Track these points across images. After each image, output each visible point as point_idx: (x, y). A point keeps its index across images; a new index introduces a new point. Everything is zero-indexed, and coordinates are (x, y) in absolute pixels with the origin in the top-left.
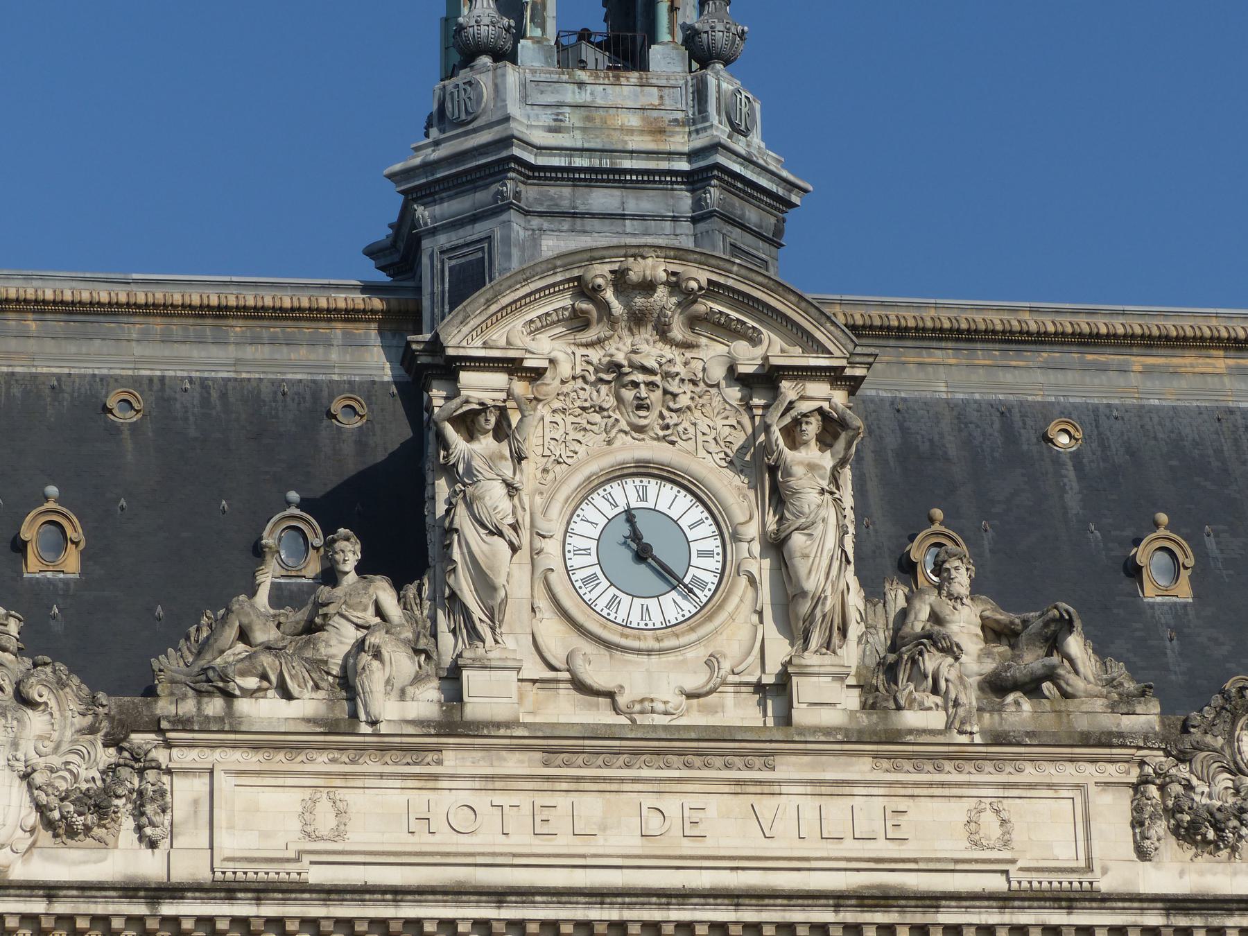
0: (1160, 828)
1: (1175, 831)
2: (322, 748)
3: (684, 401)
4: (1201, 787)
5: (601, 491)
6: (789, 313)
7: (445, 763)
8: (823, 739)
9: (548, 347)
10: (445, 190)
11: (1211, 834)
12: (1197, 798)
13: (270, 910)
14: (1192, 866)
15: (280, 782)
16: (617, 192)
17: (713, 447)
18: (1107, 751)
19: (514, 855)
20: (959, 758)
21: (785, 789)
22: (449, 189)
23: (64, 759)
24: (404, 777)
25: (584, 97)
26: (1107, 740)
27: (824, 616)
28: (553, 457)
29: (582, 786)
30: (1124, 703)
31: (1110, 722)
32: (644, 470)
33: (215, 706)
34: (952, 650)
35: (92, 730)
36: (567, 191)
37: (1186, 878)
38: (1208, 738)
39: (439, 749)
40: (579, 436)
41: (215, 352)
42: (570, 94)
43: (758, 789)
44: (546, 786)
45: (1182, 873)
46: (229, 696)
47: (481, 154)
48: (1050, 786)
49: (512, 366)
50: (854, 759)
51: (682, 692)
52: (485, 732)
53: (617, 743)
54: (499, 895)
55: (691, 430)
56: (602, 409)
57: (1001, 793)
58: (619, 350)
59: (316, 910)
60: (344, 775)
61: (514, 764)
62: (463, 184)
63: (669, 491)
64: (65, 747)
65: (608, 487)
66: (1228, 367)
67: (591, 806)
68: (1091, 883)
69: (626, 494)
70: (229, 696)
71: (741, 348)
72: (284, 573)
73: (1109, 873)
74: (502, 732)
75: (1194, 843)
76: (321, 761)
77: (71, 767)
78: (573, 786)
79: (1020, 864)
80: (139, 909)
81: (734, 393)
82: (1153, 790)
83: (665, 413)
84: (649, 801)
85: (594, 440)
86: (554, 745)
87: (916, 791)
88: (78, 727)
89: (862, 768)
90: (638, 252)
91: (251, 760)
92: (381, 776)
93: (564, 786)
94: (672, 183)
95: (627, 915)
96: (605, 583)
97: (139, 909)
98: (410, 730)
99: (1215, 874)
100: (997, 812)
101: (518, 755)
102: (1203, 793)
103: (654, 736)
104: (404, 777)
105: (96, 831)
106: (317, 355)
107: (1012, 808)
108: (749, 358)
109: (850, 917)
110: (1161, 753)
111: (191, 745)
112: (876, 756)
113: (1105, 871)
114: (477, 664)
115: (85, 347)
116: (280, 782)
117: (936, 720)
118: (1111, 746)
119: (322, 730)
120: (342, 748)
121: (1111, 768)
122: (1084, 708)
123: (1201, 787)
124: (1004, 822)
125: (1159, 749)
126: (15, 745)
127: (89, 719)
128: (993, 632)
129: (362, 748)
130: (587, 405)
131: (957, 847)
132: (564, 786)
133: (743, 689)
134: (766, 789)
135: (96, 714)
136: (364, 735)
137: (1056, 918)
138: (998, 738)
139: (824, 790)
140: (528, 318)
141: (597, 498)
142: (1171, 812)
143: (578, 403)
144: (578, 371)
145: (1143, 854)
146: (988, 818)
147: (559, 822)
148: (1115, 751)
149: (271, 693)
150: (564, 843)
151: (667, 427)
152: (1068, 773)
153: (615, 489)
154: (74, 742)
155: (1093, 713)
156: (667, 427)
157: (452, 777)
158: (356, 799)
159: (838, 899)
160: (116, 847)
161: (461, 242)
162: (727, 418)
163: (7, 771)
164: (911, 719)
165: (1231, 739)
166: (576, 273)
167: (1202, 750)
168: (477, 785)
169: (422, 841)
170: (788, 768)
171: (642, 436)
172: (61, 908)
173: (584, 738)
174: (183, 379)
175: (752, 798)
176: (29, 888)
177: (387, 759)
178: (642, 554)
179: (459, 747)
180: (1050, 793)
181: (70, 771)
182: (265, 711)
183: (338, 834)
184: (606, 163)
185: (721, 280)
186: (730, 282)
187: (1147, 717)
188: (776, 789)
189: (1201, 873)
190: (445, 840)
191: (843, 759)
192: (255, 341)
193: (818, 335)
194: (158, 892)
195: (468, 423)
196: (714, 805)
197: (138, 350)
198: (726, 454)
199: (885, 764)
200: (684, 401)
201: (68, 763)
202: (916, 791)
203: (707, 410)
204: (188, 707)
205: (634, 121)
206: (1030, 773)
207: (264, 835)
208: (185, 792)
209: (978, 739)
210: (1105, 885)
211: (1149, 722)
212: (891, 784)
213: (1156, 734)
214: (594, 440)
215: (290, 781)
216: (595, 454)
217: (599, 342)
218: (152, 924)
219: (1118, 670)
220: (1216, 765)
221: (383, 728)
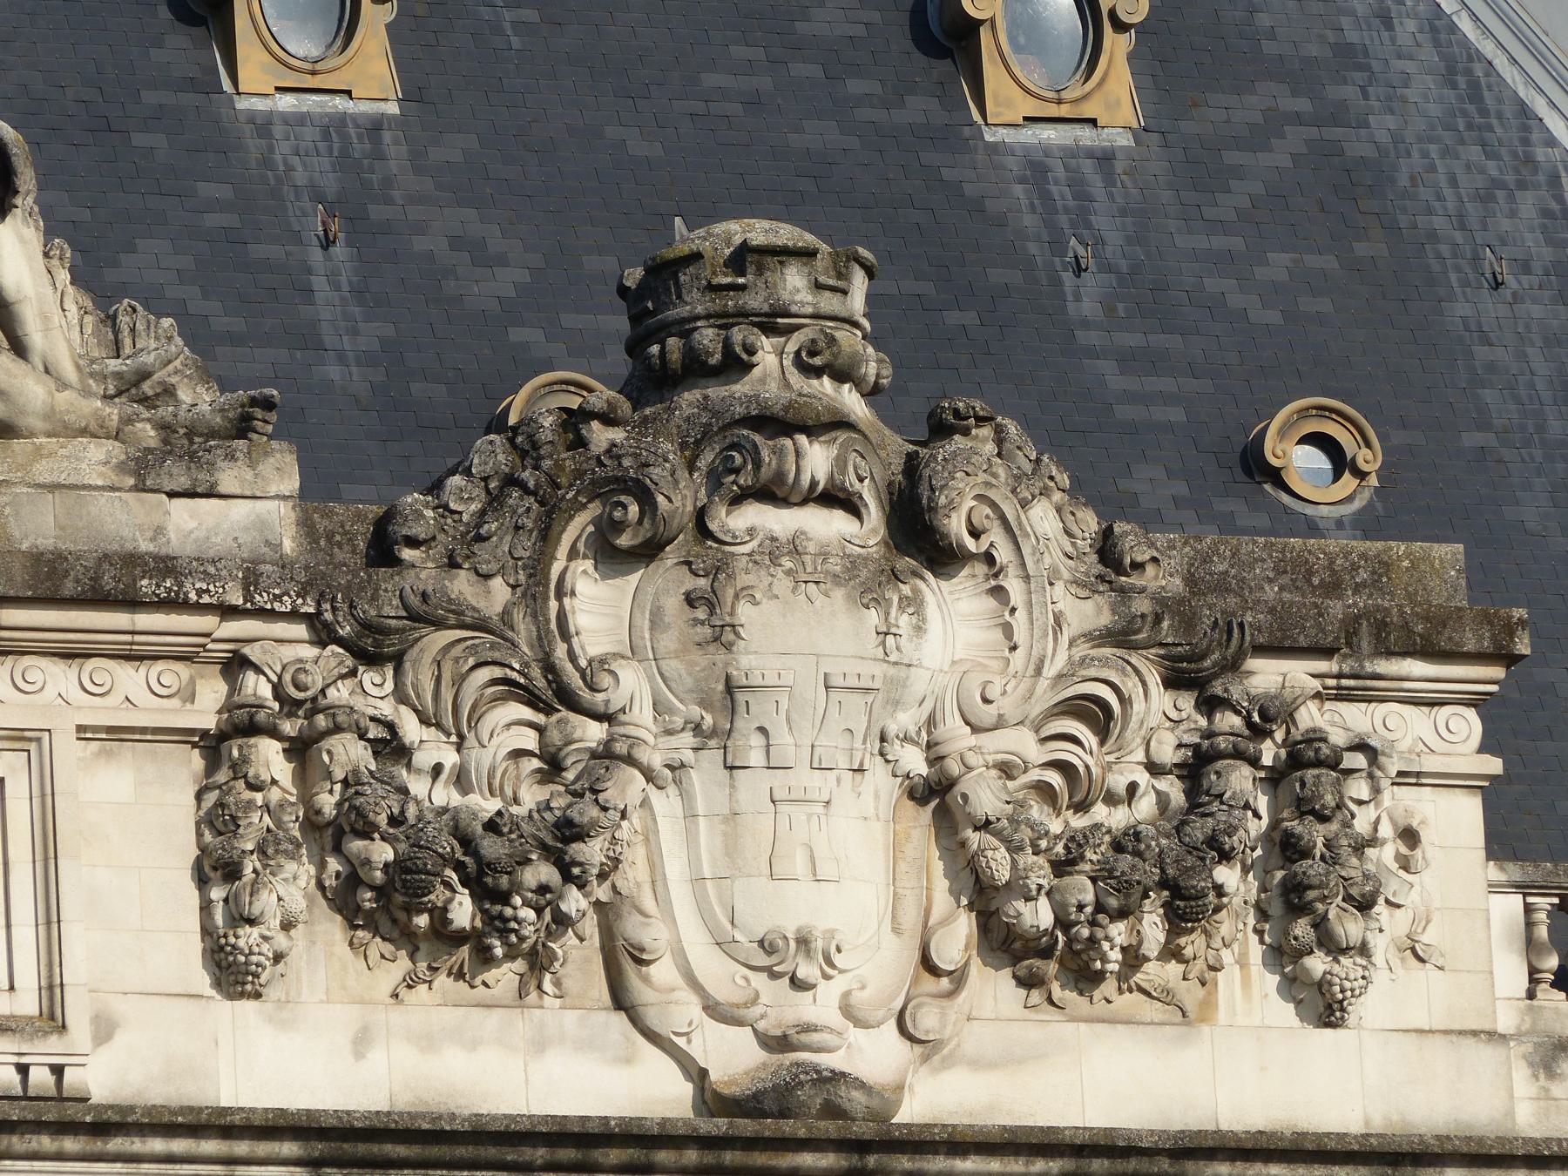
0: (292, 886)
1: (344, 898)
4: (433, 748)
11: (463, 911)
12: (418, 786)
14: (397, 1015)
18: (120, 619)
30: (179, 457)
37: (377, 1057)
38: (462, 585)
45: (361, 1042)
68: (58, 1070)
73: (120, 1038)
75: (407, 939)
82: (270, 758)
99: (473, 1045)
102: (437, 770)
110: (300, 630)
113: (104, 1030)
118: (133, 603)
121: (130, 678)
122: (44, 471)
123: (433, 748)
125: (294, 616)
142: (329, 835)
145: (232, 973)
148: (145, 620)
165: (536, 586)
167: (439, 624)
187: (253, 508)
189: (428, 1042)
210: (103, 1078)
211: (261, 524)
213: (283, 564)
219: (157, 344)
220: (485, 674)
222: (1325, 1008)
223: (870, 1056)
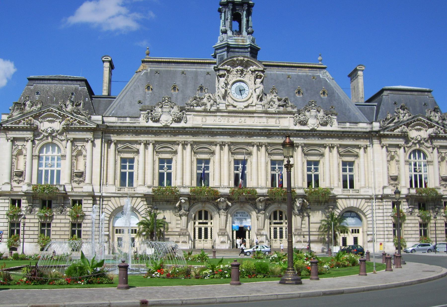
25: (236, 38)
26: (290, 113)
33: (192, 107)
34: (274, 102)
42: (234, 38)
46: (193, 106)
49: (225, 70)
63: (243, 83)
67: (233, 119)
69: (238, 84)
70: (193, 106)
76: (204, 114)
81: (250, 72)
86: (229, 112)
89: (263, 115)
90: (239, 56)
106: (205, 67)
107: (281, 120)
115: (179, 67)
117: (272, 110)
128: (279, 100)
141: (235, 84)
146: (278, 121)
150: (230, 123)
153: (237, 83)
155: (289, 109)
158: (208, 118)
159: (260, 130)
164: (269, 110)
169: (215, 123)
176: (172, 127)
183: (205, 122)
194: (185, 128)
195: (221, 76)
196: (248, 119)
197: (185, 67)
204: (189, 108)
205: (241, 41)
206: (282, 116)
208: (188, 117)
210: (290, 128)
222: (331, 126)
223: (316, 128)
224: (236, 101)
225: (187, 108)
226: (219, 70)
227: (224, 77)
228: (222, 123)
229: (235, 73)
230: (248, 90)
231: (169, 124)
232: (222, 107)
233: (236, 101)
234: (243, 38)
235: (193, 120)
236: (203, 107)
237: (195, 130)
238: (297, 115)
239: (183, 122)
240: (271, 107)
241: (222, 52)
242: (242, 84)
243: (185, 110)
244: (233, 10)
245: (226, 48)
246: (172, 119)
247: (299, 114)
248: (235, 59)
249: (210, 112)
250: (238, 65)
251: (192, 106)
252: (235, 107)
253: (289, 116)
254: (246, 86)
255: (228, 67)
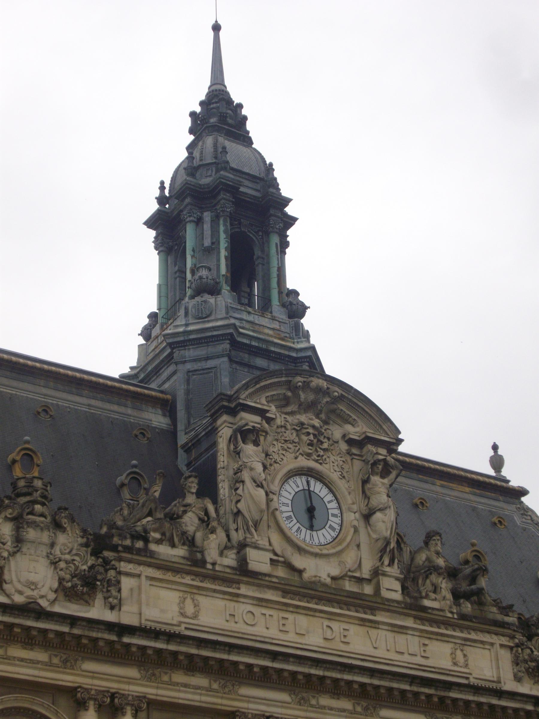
2: (188, 573)
3: (325, 446)
5: (292, 479)
6: (373, 415)
7: (241, 589)
8: (396, 605)
9: (273, 410)
10: (192, 345)
13: (172, 647)
15: (170, 586)
16: (266, 360)
17: (336, 468)
19: (273, 639)
20: (447, 623)
21: (381, 626)
22: (194, 345)
23: (72, 558)
24: (225, 593)
27: (390, 551)
28: (273, 460)
29: (299, 610)
31: (500, 617)
32: (309, 473)
33: (140, 544)
35: (86, 545)
36: (246, 356)
39: (238, 582)
40: (284, 452)
41: (78, 399)
43: (370, 624)
44: (284, 608)
46: (146, 541)
47: (215, 330)
48: (482, 642)
50: (407, 617)
51: (329, 575)
52: (260, 577)
53: (313, 592)
54: (274, 656)
55: (328, 459)
56: (294, 442)
57: (463, 642)
58: (303, 418)
59: (194, 651)
60: (198, 588)
61: (270, 595)
62: (201, 343)
64: (74, 552)
65: (295, 478)
66: (470, 491)
67: (303, 621)
71: (349, 428)
72: (131, 498)
74: (267, 578)
76: (188, 580)
77: (75, 562)
78: (295, 610)
79: (474, 675)
80: (114, 638)
81: (344, 446)
83: (319, 449)
84: (326, 623)
85: (290, 456)
87: (431, 636)
88: (79, 542)
89: (409, 622)
91: (158, 574)
92: (215, 591)
93: (291, 609)
94: (288, 361)
95: (328, 674)
96: (295, 521)
97: (114, 638)
98: (228, 570)
100: (462, 650)
101: (271, 591)
103: (329, 591)
104: (225, 593)
105: (86, 597)
108: (355, 431)
109: (415, 689)
111: (130, 561)
112: (415, 617)
114: (253, 545)
115: (21, 385)
116: (170, 586)
119: (189, 563)
120: (196, 574)
124: (465, 656)
126: (52, 545)
127: (85, 540)
129: (205, 577)
130: (287, 439)
131: (446, 664)
132: (291, 609)
133: (353, 579)
134: (373, 625)
135: (88, 538)
136: (208, 569)
137: (495, 701)
138: (463, 617)
139: (396, 629)
140: (267, 394)
143: (283, 438)
144: (283, 424)
147: (289, 627)
148: (506, 631)
149: (164, 543)
150: (291, 637)
151: (318, 456)
152: (486, 638)
154: (77, 550)
155: (493, 613)
156: (318, 456)
157: (245, 596)
158: (203, 601)
159: (413, 679)
160: (94, 606)
161: (200, 368)
162: (341, 457)
163: (46, 559)
166: (290, 379)
168: (255, 602)
169: (231, 626)
170: (380, 617)
171: (308, 458)
172: (76, 631)
173: (300, 587)
174: (66, 407)
175: (367, 629)
177: (216, 583)
178: (311, 511)
179: (247, 583)
180: (482, 646)
181: (74, 564)
182: (164, 550)
183: (195, 616)
184: (264, 346)
185: (346, 395)
186: (350, 397)
188: (377, 626)
190: (241, 627)
191: (402, 617)
192: (94, 398)
193: (384, 427)
195: (246, 434)
198: (342, 473)
199: (418, 622)
200: (325, 446)
201: (74, 560)
202: (431, 636)
203: (334, 452)
204: (128, 542)
206: (473, 636)
207: (162, 611)
208: (126, 583)
209: (456, 616)
212: (422, 631)
214: (290, 456)
215: (174, 587)
216: (290, 462)
217: (292, 413)
218: (118, 646)
221: (217, 568)
224: (300, 550)
225: (116, 540)
226: (233, 412)
227: (256, 443)
228: (259, 630)
229: (291, 435)
230: (337, 512)
231: (44, 603)
232: (258, 561)
233: (300, 550)
234: (276, 325)
235: (152, 600)
236: (180, 552)
237: (160, 645)
238: (525, 639)
239: (99, 600)
240: (433, 596)
241: (207, 359)
242: (317, 487)
243: (114, 548)
244: (233, 219)
245: (226, 345)
246: (56, 585)
247: (530, 638)
248: (299, 380)
249: (215, 578)
250: (309, 407)
251: (136, 537)
252: (300, 572)
253: (495, 639)
254: (330, 497)
255: (273, 410)
